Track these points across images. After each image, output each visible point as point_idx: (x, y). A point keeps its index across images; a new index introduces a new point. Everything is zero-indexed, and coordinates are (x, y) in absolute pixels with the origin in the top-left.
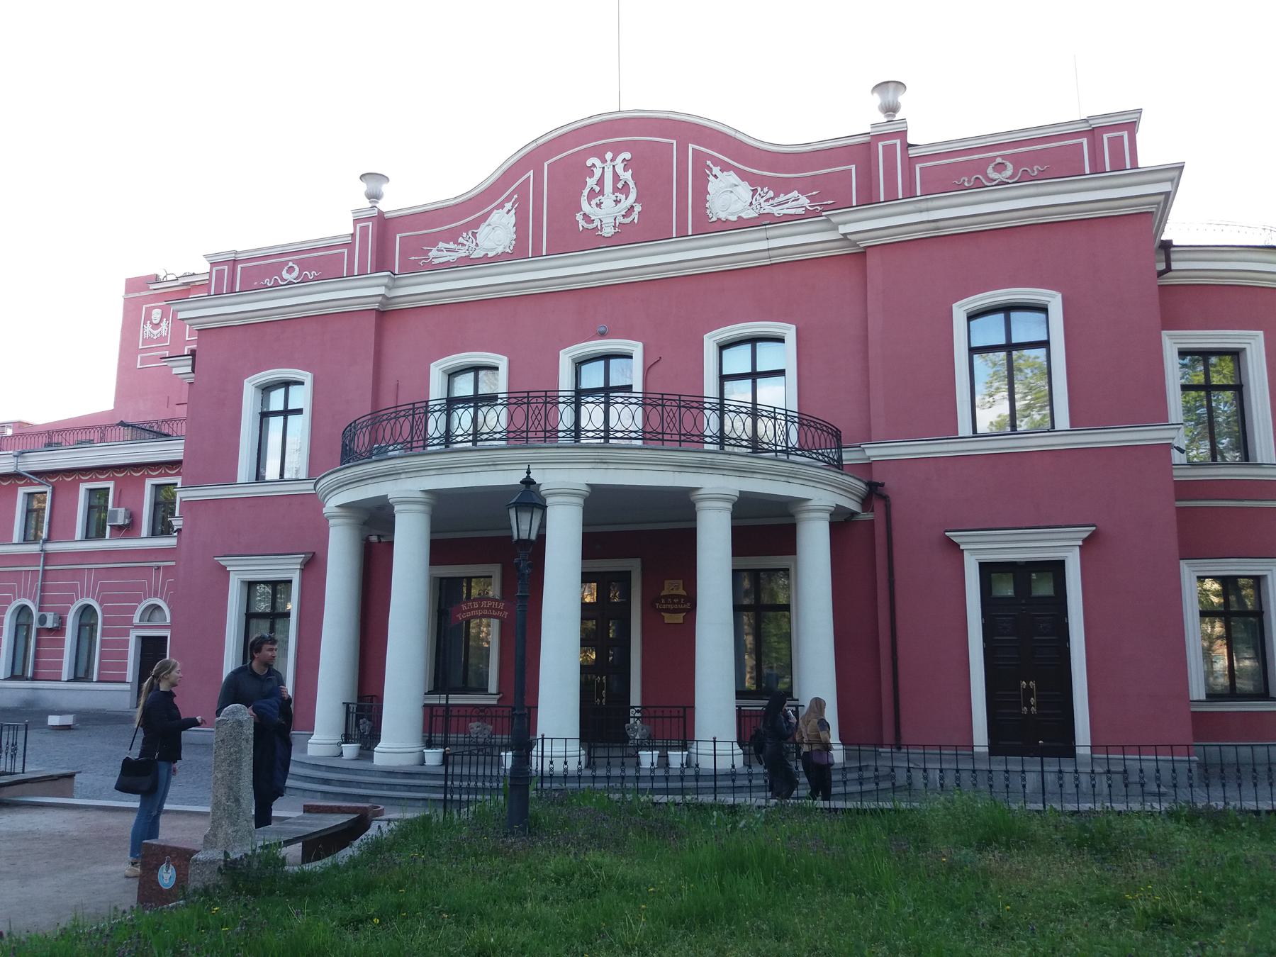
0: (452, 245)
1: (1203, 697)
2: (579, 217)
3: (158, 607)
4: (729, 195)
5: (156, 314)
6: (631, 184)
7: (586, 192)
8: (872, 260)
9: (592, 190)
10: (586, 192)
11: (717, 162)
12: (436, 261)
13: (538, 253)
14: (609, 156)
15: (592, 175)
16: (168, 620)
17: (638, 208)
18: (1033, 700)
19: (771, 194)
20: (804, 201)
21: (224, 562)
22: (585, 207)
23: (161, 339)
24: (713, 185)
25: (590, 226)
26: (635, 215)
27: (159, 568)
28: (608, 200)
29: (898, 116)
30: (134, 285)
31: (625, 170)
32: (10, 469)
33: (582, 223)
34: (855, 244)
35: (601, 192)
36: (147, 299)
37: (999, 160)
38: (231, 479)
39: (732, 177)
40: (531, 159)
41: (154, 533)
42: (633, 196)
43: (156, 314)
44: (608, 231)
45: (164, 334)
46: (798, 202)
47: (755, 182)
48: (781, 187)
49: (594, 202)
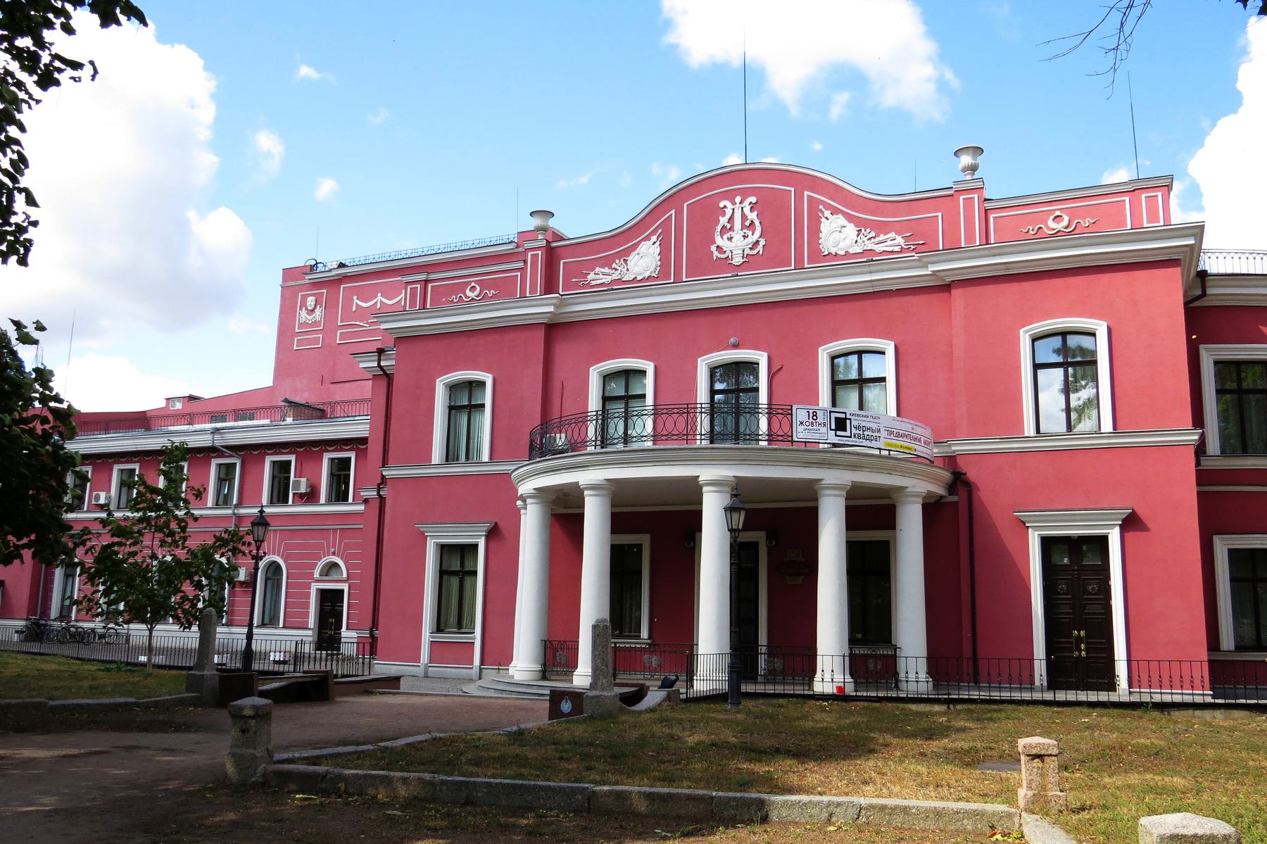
0: (606, 270)
1: (1232, 647)
2: (713, 248)
3: (335, 565)
4: (838, 234)
6: (757, 223)
7: (719, 228)
9: (724, 227)
10: (719, 228)
11: (828, 207)
12: (593, 283)
13: (678, 280)
14: (738, 199)
15: (724, 214)
16: (345, 575)
17: (762, 242)
18: (1083, 646)
19: (873, 234)
20: (900, 240)
21: (422, 527)
22: (719, 241)
23: (316, 323)
24: (825, 227)
25: (723, 256)
26: (760, 248)
27: (335, 530)
28: (737, 235)
29: (977, 174)
30: (288, 274)
31: (752, 210)
32: (209, 444)
33: (716, 254)
34: (941, 278)
35: (731, 229)
36: (301, 288)
37: (1058, 213)
38: (425, 459)
39: (841, 220)
40: (672, 199)
41: (330, 501)
42: (758, 233)
43: (311, 301)
44: (738, 260)
45: (318, 318)
46: (894, 241)
47: (860, 224)
48: (880, 228)
49: (725, 237)
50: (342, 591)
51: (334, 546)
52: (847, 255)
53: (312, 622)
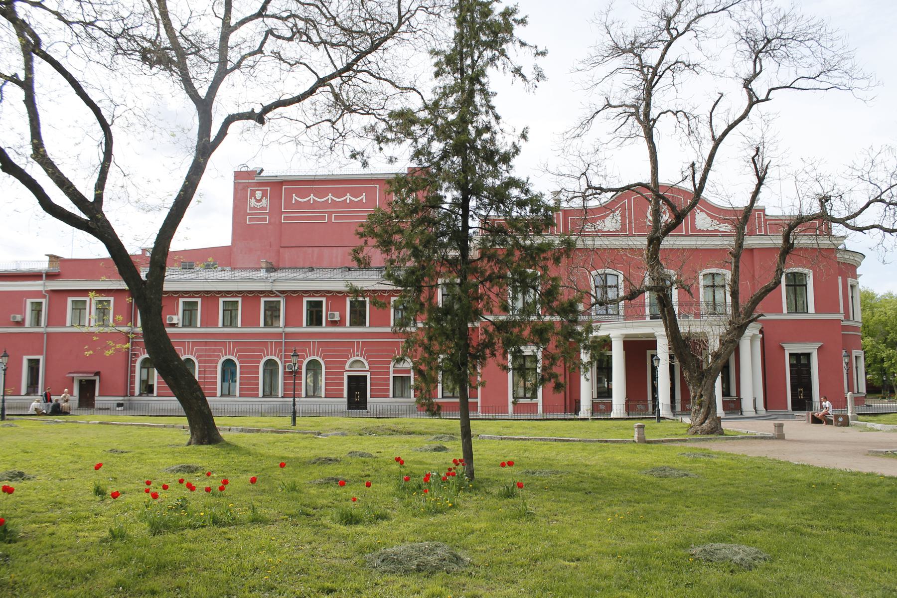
5: (258, 194)
8: (755, 253)
23: (262, 208)
39: (704, 215)
41: (352, 324)
43: (258, 194)
45: (264, 205)
47: (712, 217)
48: (723, 221)
50: (366, 377)
51: (358, 351)
52: (707, 231)
53: (345, 394)
